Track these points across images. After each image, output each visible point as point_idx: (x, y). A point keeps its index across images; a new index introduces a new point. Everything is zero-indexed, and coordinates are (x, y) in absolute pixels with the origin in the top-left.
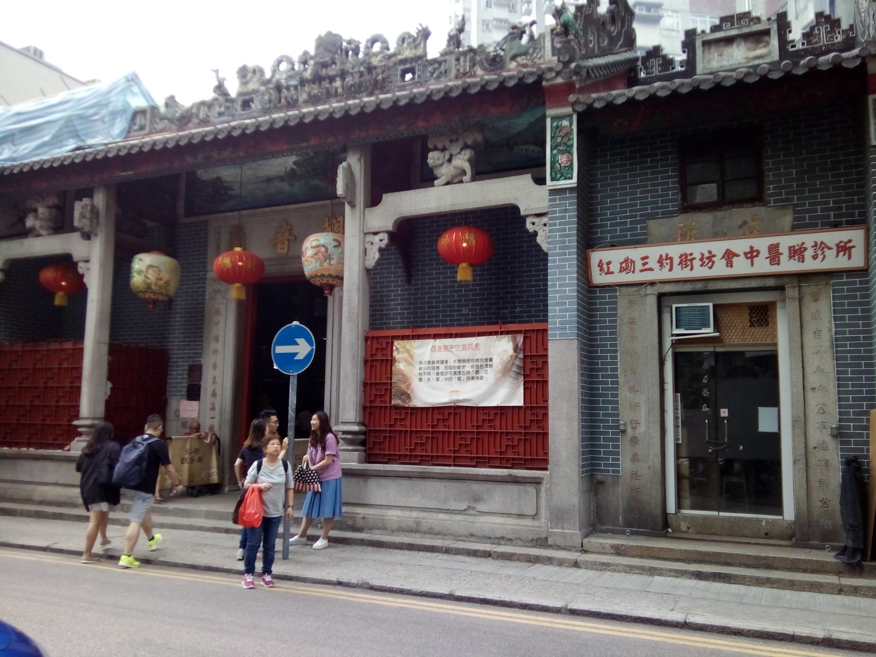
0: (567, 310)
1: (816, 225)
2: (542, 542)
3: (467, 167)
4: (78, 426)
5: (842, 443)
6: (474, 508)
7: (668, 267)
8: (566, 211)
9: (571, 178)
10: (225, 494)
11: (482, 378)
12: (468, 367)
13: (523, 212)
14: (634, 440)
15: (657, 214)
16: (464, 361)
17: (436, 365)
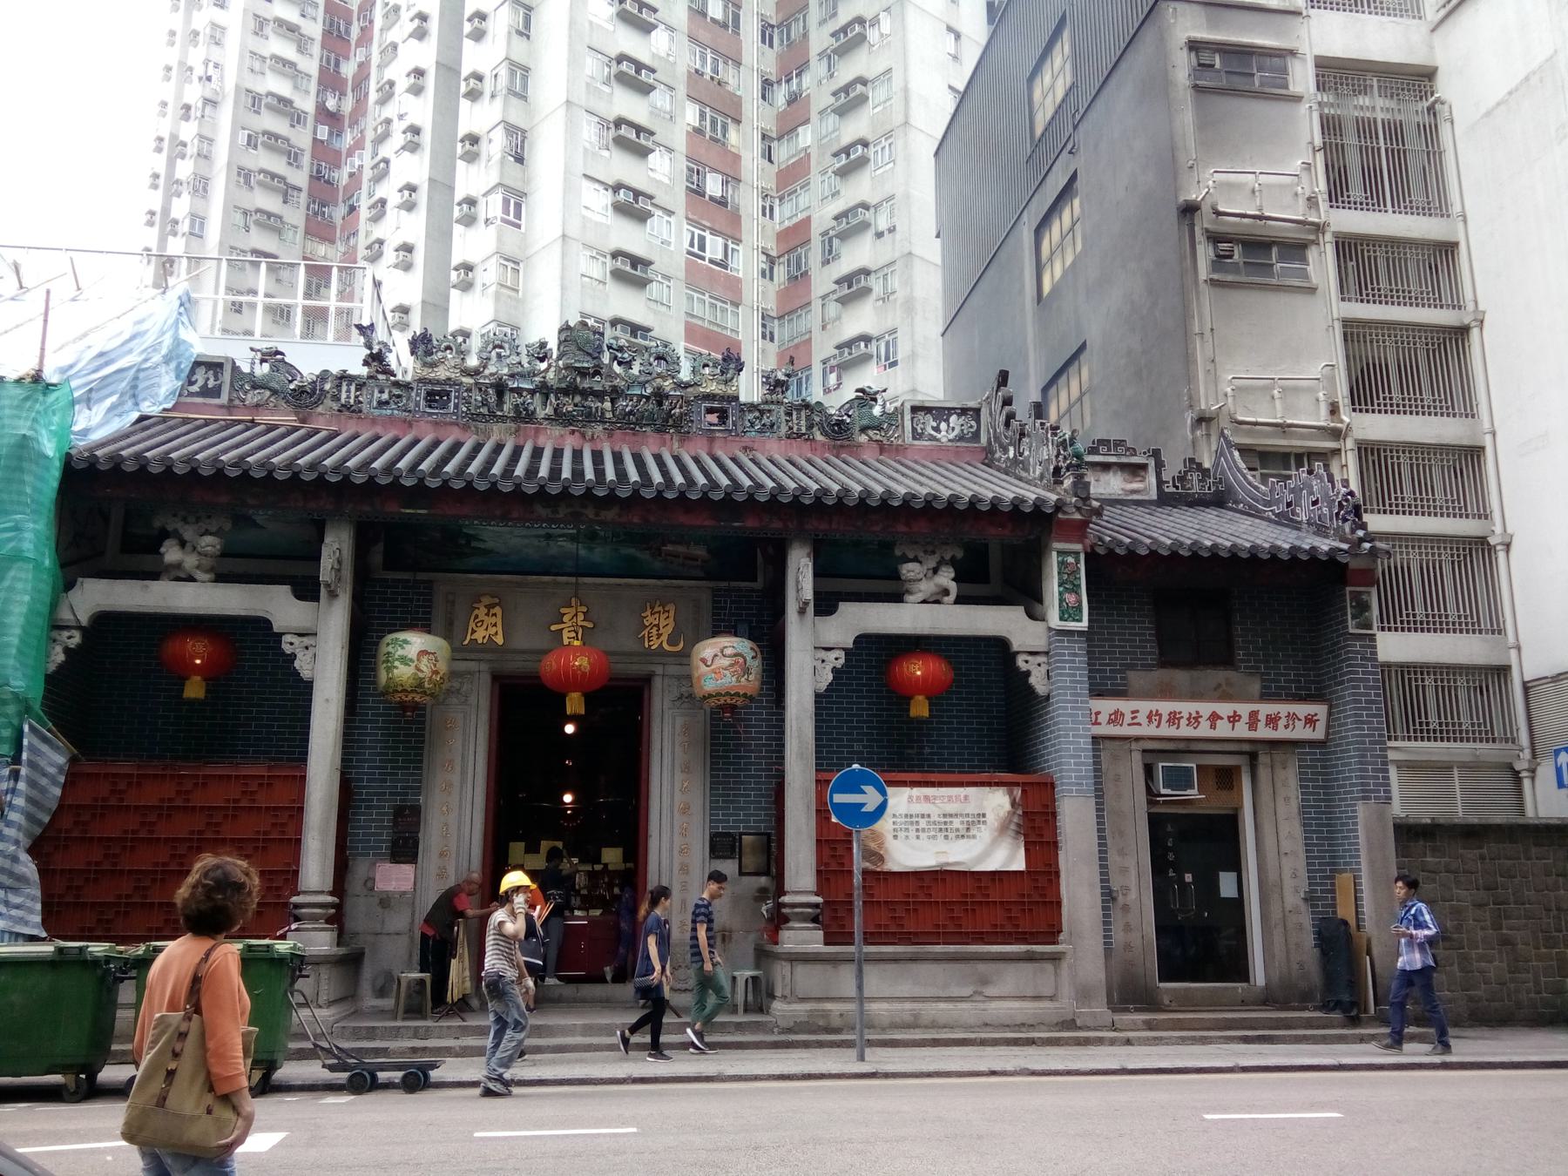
0: (1083, 764)
1: (1280, 695)
2: (1070, 1024)
3: (953, 587)
4: (297, 906)
5: (1313, 906)
6: (980, 993)
7: (1156, 723)
8: (1075, 655)
9: (1061, 619)
10: (473, 1011)
11: (974, 837)
12: (957, 823)
13: (1015, 647)
14: (1126, 908)
15: (1137, 665)
16: (951, 816)
17: (914, 819)
